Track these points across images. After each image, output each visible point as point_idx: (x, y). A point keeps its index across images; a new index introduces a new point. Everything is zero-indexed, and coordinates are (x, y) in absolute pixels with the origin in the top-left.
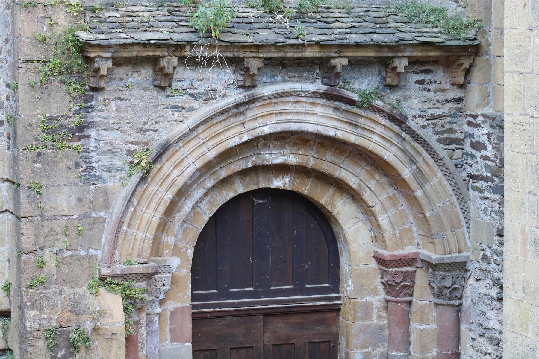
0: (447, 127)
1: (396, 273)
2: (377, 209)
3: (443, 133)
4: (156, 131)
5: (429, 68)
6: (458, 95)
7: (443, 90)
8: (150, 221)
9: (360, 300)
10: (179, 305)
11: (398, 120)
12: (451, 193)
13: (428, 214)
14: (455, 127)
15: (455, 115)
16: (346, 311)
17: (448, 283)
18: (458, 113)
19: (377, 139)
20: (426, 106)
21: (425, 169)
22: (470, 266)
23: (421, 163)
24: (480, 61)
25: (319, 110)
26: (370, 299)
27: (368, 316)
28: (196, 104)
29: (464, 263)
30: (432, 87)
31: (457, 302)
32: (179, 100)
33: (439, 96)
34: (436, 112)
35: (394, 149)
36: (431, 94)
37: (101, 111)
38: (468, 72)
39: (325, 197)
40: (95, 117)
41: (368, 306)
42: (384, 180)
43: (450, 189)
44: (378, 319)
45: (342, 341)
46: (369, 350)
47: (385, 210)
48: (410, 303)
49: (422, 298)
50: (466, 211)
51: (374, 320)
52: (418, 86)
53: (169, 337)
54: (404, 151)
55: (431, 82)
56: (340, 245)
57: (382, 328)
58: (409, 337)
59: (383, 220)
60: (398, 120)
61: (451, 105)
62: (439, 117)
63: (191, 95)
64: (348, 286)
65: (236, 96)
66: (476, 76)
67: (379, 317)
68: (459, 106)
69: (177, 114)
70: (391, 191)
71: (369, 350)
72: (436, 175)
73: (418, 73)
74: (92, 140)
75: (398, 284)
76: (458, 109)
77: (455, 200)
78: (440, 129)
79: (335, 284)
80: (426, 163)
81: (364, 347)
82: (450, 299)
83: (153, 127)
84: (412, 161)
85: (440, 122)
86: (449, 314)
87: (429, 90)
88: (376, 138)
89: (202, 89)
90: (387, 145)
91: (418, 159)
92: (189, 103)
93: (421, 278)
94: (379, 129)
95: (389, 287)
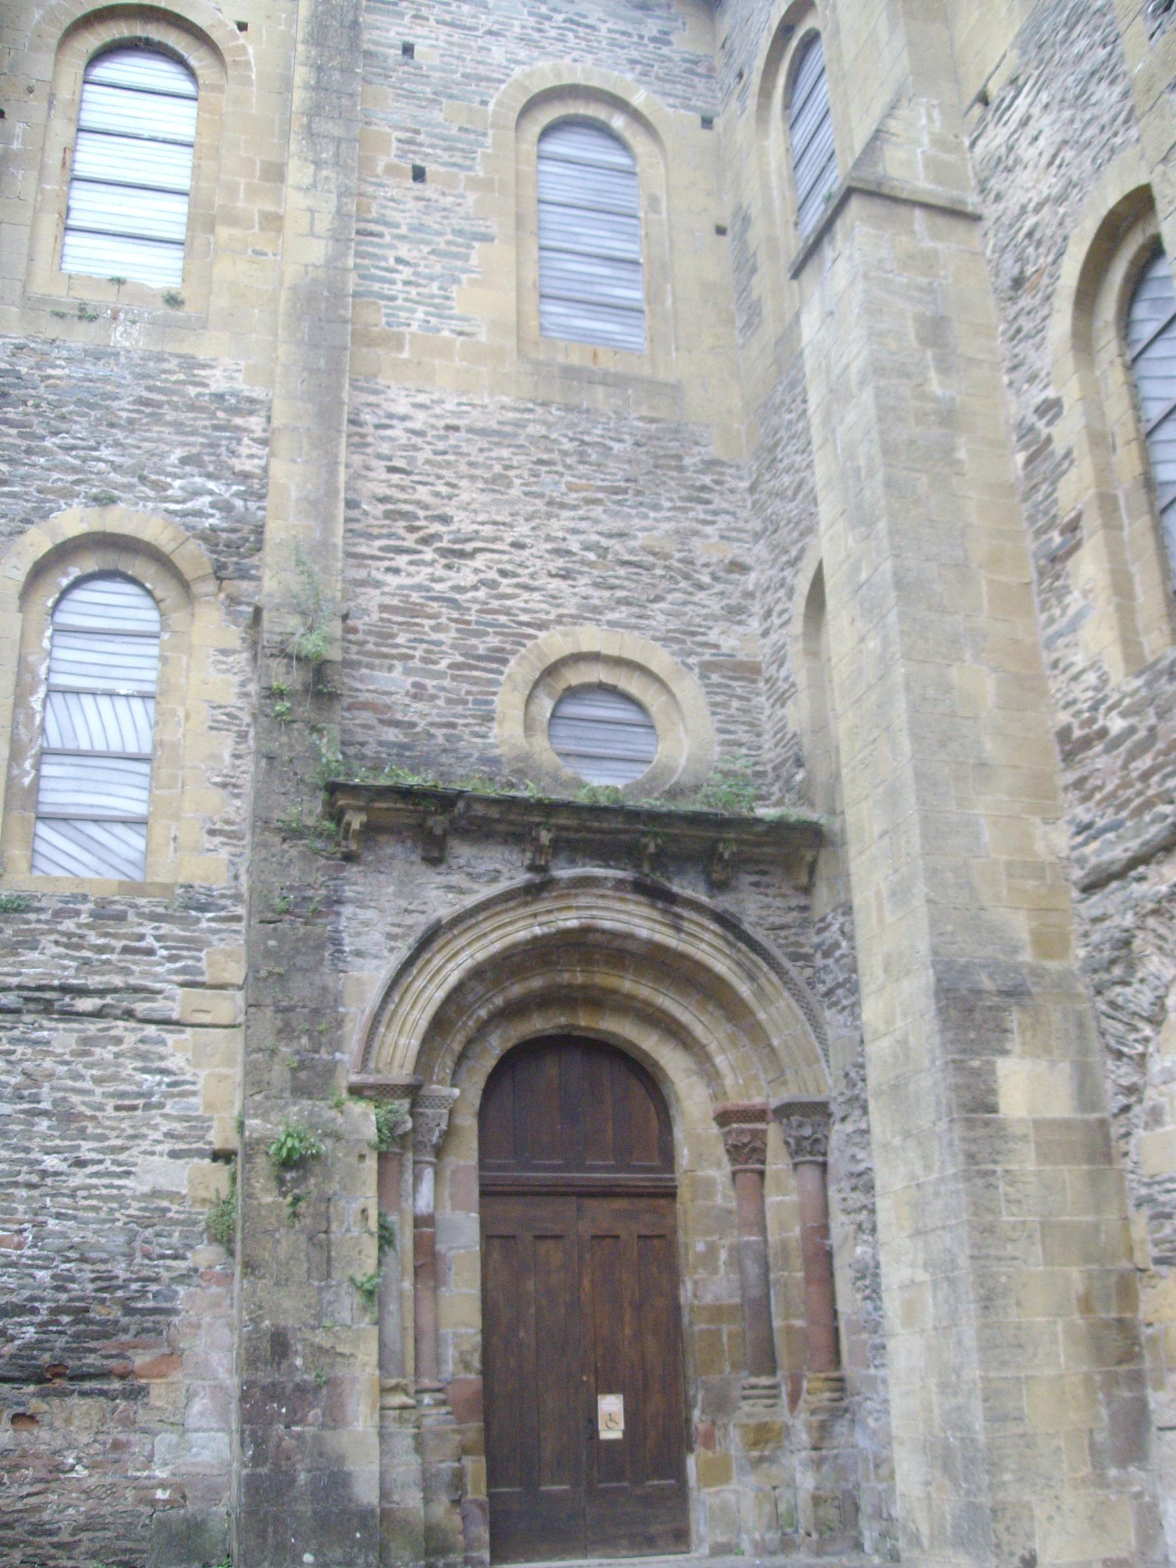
0: (792, 939)
1: (742, 1132)
2: (713, 1047)
3: (788, 945)
4: (423, 912)
5: (764, 867)
6: (803, 902)
7: (784, 896)
8: (416, 1024)
9: (700, 1173)
10: (462, 1163)
11: (728, 923)
12: (803, 1017)
13: (776, 1042)
14: (802, 939)
15: (801, 926)
16: (684, 1193)
17: (807, 1131)
18: (805, 924)
19: (706, 948)
20: (764, 913)
21: (768, 989)
22: (833, 1107)
23: (762, 981)
24: (824, 855)
25: (631, 907)
26: (712, 1172)
27: (710, 1194)
28: (476, 886)
29: (825, 1105)
30: (770, 891)
31: (820, 1159)
32: (455, 879)
33: (778, 902)
34: (778, 921)
35: (728, 962)
36: (770, 899)
37: (356, 884)
38: (812, 868)
39: (650, 1043)
40: (349, 892)
41: (710, 1183)
42: (718, 1013)
43: (800, 1013)
44: (724, 1197)
45: (681, 1232)
46: (715, 1238)
47: (723, 1050)
48: (762, 1174)
49: (777, 1162)
50: (822, 1040)
51: (719, 1200)
52: (753, 889)
53: (448, 1204)
54: (739, 964)
55: (768, 886)
56: (673, 1112)
57: (729, 1212)
58: (764, 1218)
59: (720, 1061)
60: (728, 923)
61: (795, 914)
62: (782, 927)
63: (469, 874)
64: (684, 1156)
65: (523, 877)
66: (822, 869)
67: (725, 1196)
68: (805, 915)
69: (451, 896)
70: (729, 1028)
71: (715, 1238)
72: (781, 995)
73: (751, 874)
74: (343, 919)
75: (745, 1145)
76: (805, 920)
77: (809, 1029)
78: (783, 942)
79: (673, 1172)
80: (768, 979)
81: (708, 1233)
82: (811, 1153)
83: (422, 908)
84: (752, 978)
85: (783, 933)
86: (810, 1175)
87: (767, 895)
88: (703, 946)
89: (481, 869)
90: (719, 956)
91: (758, 974)
92: (466, 883)
93: (774, 1133)
94: (707, 936)
95: (735, 1152)
